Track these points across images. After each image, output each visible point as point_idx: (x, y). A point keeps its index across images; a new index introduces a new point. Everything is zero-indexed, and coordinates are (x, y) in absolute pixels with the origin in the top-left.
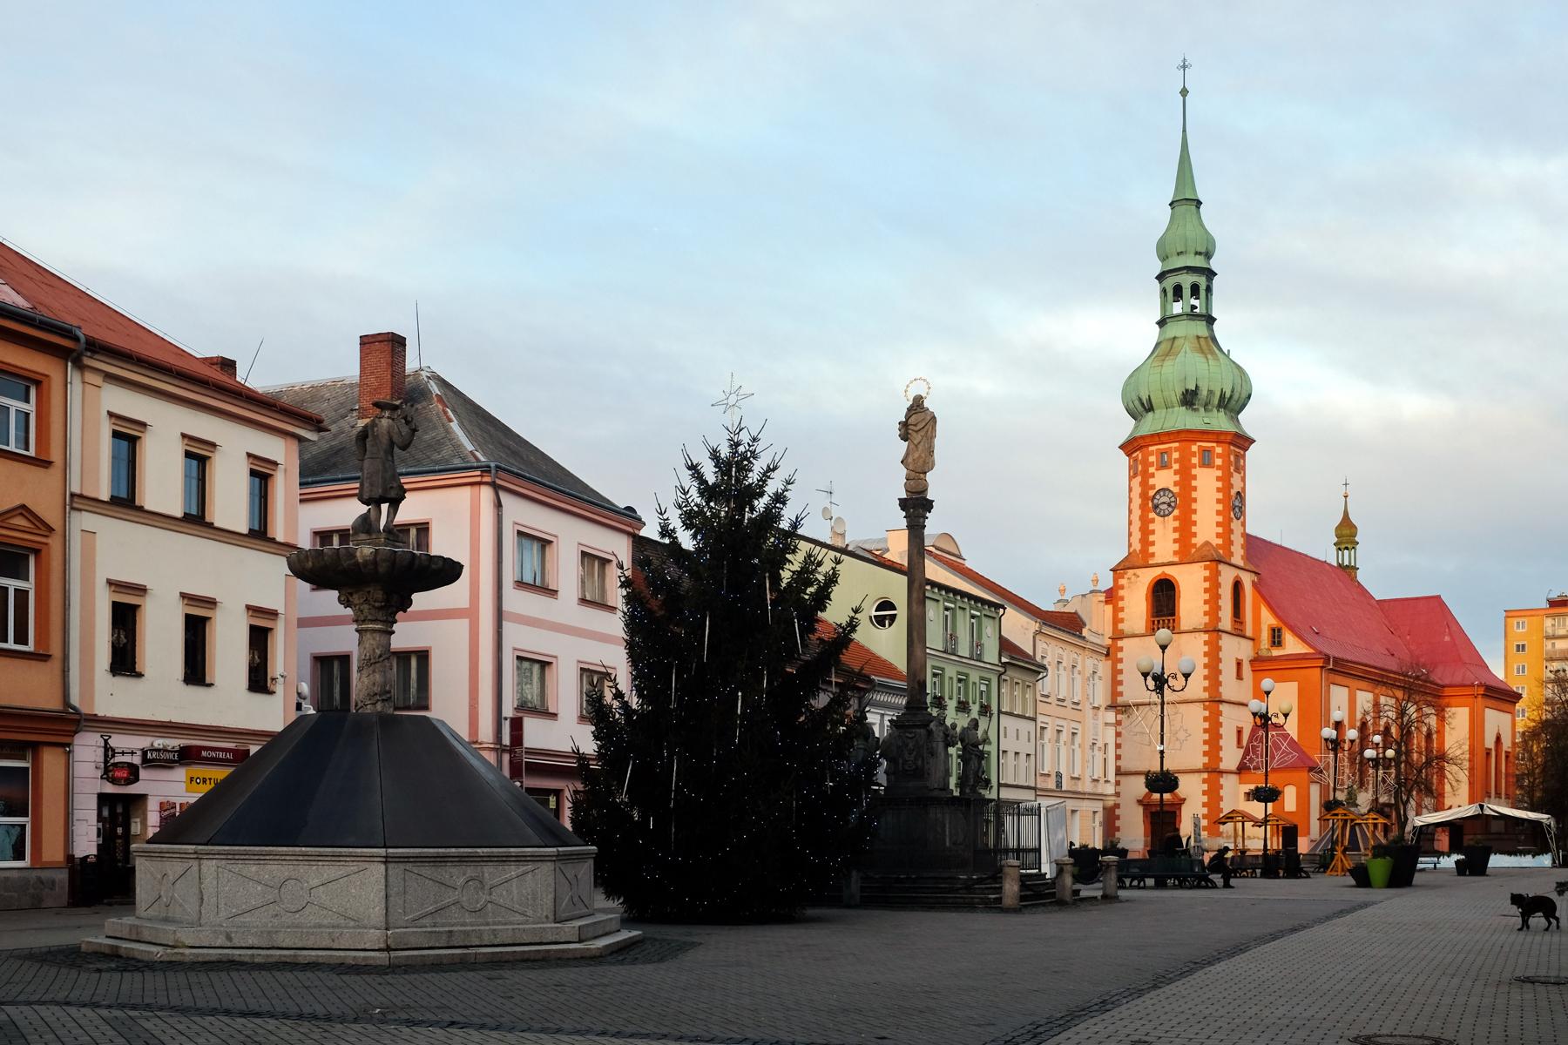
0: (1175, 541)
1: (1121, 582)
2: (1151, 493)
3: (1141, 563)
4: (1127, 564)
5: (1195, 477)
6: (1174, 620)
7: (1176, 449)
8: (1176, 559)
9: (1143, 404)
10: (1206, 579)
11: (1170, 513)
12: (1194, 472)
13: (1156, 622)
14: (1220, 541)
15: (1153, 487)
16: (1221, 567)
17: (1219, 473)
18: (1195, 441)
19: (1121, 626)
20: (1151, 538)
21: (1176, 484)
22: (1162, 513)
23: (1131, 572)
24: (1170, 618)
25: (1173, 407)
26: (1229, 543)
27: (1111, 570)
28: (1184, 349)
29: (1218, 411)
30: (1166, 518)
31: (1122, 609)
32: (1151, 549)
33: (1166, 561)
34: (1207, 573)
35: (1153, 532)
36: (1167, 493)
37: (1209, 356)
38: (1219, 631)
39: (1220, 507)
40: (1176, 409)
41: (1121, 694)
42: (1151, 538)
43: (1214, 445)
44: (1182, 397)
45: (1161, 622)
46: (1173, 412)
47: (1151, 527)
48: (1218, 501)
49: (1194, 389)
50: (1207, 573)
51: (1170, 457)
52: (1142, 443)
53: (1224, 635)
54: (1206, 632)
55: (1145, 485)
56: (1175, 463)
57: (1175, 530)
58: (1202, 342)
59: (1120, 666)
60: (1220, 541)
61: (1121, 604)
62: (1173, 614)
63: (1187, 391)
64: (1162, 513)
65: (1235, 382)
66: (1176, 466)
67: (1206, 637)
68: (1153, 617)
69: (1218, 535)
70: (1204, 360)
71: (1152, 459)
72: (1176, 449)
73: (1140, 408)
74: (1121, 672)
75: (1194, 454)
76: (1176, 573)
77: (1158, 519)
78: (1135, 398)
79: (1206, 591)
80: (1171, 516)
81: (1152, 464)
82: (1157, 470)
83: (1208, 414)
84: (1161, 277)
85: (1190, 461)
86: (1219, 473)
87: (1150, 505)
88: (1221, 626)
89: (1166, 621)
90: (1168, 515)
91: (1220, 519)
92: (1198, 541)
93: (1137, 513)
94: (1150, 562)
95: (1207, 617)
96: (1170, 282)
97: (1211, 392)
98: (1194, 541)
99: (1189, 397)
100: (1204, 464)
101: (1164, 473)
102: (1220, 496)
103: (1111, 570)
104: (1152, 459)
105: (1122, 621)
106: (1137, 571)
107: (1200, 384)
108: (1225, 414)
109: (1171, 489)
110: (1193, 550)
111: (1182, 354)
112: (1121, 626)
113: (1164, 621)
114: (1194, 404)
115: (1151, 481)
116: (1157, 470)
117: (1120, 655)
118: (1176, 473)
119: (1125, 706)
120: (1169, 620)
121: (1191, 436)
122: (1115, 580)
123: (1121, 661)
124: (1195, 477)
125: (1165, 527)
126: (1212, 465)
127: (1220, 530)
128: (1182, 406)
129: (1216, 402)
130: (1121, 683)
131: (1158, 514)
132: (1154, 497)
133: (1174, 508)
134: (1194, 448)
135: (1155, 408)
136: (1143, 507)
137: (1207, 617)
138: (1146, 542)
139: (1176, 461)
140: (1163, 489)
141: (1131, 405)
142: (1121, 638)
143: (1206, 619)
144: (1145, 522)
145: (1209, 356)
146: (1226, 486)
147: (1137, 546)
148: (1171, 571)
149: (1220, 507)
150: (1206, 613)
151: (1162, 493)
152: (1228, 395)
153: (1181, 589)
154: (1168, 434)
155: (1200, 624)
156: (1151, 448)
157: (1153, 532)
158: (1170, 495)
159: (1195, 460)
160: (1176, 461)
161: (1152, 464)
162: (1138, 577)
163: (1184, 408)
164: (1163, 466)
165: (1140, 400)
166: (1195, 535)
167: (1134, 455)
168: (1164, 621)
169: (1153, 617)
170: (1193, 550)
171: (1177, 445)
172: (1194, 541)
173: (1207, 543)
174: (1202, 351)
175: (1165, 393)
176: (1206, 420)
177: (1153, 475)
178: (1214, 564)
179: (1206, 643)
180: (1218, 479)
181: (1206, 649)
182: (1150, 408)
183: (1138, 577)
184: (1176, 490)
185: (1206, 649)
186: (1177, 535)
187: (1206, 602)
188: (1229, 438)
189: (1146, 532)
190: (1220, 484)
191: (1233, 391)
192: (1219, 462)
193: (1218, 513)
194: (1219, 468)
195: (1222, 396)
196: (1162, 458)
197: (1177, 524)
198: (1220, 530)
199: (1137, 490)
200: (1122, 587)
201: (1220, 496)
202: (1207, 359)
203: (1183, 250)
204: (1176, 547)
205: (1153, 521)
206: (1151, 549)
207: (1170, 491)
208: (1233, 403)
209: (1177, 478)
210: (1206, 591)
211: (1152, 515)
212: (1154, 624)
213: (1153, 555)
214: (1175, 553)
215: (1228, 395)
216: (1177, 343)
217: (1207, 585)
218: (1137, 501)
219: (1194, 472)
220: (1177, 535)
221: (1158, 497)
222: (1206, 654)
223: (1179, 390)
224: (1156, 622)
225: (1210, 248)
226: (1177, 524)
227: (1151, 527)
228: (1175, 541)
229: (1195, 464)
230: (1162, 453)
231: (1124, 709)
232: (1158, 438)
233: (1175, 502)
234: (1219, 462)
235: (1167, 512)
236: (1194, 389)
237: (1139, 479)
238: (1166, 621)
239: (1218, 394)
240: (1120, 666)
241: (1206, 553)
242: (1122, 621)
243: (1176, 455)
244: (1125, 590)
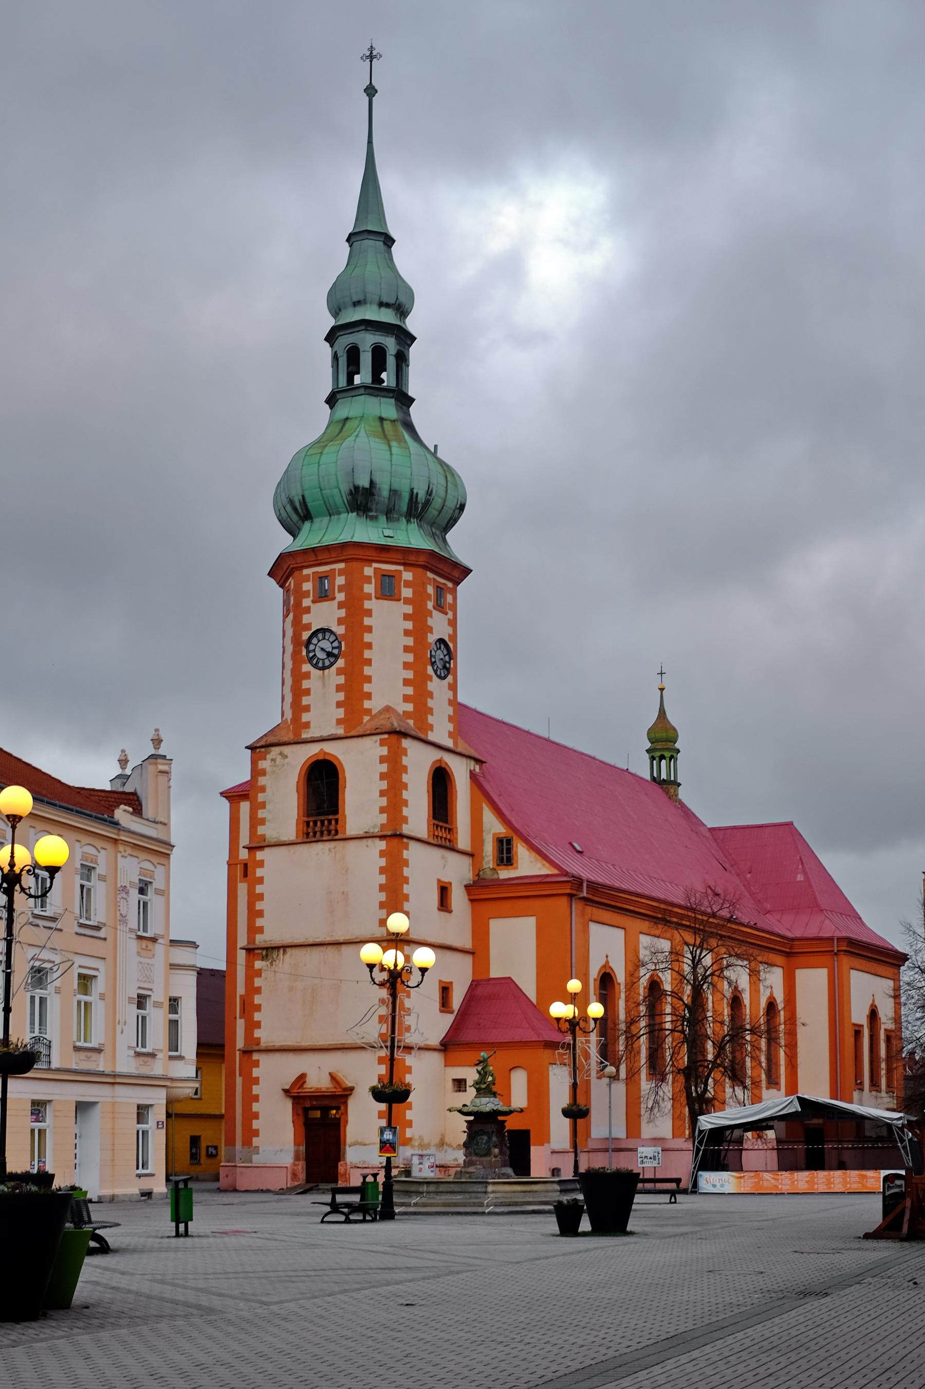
0: (339, 705)
1: (263, 764)
2: (305, 635)
3: (290, 737)
4: (271, 739)
5: (369, 613)
6: (337, 821)
7: (342, 572)
8: (340, 731)
9: (295, 509)
10: (382, 760)
11: (332, 664)
12: (367, 605)
13: (311, 824)
14: (409, 707)
15: (308, 627)
16: (406, 743)
17: (409, 609)
18: (369, 561)
19: (261, 830)
20: (305, 701)
21: (340, 621)
22: (320, 665)
23: (275, 751)
24: (330, 817)
25: (339, 513)
26: (422, 709)
27: (247, 747)
28: (356, 433)
29: (408, 521)
30: (326, 671)
31: (263, 805)
32: (305, 717)
33: (325, 733)
34: (384, 751)
35: (307, 692)
36: (327, 635)
37: (394, 444)
38: (402, 836)
39: (410, 658)
40: (344, 516)
41: (261, 930)
42: (305, 701)
43: (401, 568)
44: (349, 497)
45: (319, 824)
46: (339, 519)
47: (305, 684)
48: (407, 649)
49: (367, 485)
50: (384, 751)
51: (332, 584)
52: (292, 563)
53: (412, 845)
54: (382, 837)
55: (298, 626)
56: (340, 591)
57: (339, 688)
58: (387, 425)
59: (259, 889)
60: (409, 707)
61: (261, 797)
62: (336, 812)
63: (356, 488)
64: (320, 665)
65: (434, 481)
66: (341, 597)
67: (382, 845)
68: (308, 816)
69: (406, 699)
70: (386, 447)
71: (307, 586)
72: (342, 572)
73: (295, 517)
74: (261, 897)
75: (368, 580)
77: (315, 673)
78: (285, 501)
79: (383, 776)
80: (334, 668)
81: (306, 594)
82: (314, 602)
83: (390, 525)
84: (331, 337)
85: (362, 589)
86: (409, 609)
87: (304, 653)
88: (406, 829)
89: (326, 822)
90: (329, 667)
91: (410, 675)
92: (374, 704)
93: (289, 665)
94: (305, 736)
95: (385, 815)
96: (344, 341)
97: (394, 493)
98: (367, 704)
99: (360, 499)
100: (378, 596)
101: (325, 605)
102: (410, 641)
103: (247, 747)
104: (307, 586)
105: (263, 822)
106: (286, 750)
107: (377, 479)
108: (420, 526)
109: (334, 629)
110: (366, 718)
111: (352, 438)
112: (261, 830)
113: (322, 822)
114: (370, 510)
115: (306, 619)
116: (314, 602)
117: (259, 872)
118: (341, 605)
119: (267, 949)
120: (330, 821)
121: (360, 553)
122: (254, 763)
123: (261, 881)
124: (369, 613)
125: (324, 685)
126: (397, 597)
127: (410, 691)
128: (352, 512)
129: (404, 507)
130: (260, 914)
131: (315, 666)
132: (309, 641)
133: (336, 657)
134: (368, 571)
135: (313, 516)
136: (296, 655)
137: (385, 815)
138: (298, 708)
139: (341, 589)
140: (323, 631)
141: (284, 515)
142: (261, 848)
143: (383, 818)
144: (298, 677)
145: (394, 444)
146: (419, 629)
147: (289, 715)
148: (332, 749)
149: (410, 658)
150: (382, 810)
151: (320, 636)
152: (422, 496)
153: (347, 774)
154: (328, 548)
155: (374, 827)
156: (306, 572)
157: (307, 692)
158: (332, 638)
159: (369, 588)
160: (341, 589)
161: (306, 594)
162: (286, 757)
163: (355, 514)
164: (323, 596)
165: (291, 502)
166: (369, 696)
167: (287, 585)
168: (322, 822)
170: (366, 718)
171: (342, 565)
172: (367, 704)
173: (388, 709)
174: (385, 436)
175: (327, 492)
176: (387, 532)
177: (308, 610)
178: (394, 738)
179: (382, 854)
180: (406, 617)
181: (383, 862)
182: (307, 516)
183: (286, 757)
184: (340, 630)
185: (383, 862)
186: (341, 696)
187: (382, 793)
188: (422, 560)
189: (299, 692)
190: (409, 625)
191: (429, 493)
192: (407, 593)
193: (406, 666)
194: (407, 601)
195: (413, 497)
196: (322, 584)
197: (341, 680)
198: (410, 691)
199: (290, 632)
200: (263, 773)
201: (410, 641)
202: (390, 447)
203: (361, 298)
204: (341, 713)
205: (307, 675)
206: (305, 717)
207: (332, 632)
209: (342, 613)
210: (383, 776)
211: (306, 667)
212: (308, 825)
213: (307, 725)
214: (339, 722)
215: (422, 496)
216: (349, 425)
217: (384, 768)
218: (290, 648)
219: (367, 605)
220: (341, 696)
221: (315, 641)
222: (382, 870)
223: (345, 488)
224: (311, 824)
226: (341, 680)
227: (305, 684)
228: (339, 705)
229: (370, 595)
230: (321, 578)
231: (264, 953)
232: (316, 555)
233: (339, 647)
234: (407, 593)
235: (327, 663)
236: (367, 485)
237: (291, 616)
238: (326, 822)
239: (406, 496)
240: (259, 889)
241: (383, 722)
242: (263, 822)
243: (340, 581)
244: (267, 777)
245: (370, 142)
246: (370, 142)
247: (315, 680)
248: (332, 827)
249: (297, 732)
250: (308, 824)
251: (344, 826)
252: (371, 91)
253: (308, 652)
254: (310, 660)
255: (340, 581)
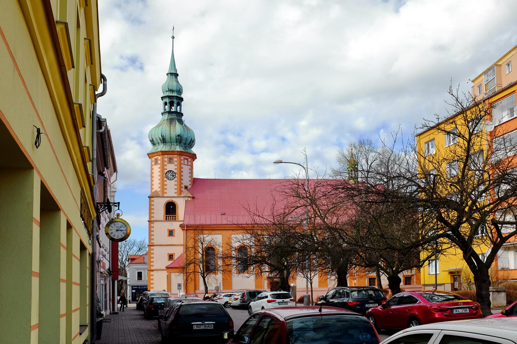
2: (166, 171)
3: (161, 195)
5: (182, 168)
6: (175, 217)
8: (176, 195)
11: (173, 179)
15: (166, 169)
21: (175, 169)
22: (170, 179)
47: (165, 183)
62: (176, 215)
71: (166, 159)
76: (176, 200)
81: (166, 161)
82: (168, 163)
90: (172, 180)
94: (165, 195)
115: (165, 167)
116: (168, 163)
118: (175, 165)
120: (173, 217)
124: (182, 168)
131: (168, 179)
132: (166, 173)
133: (175, 178)
140: (170, 171)
156: (165, 156)
161: (166, 161)
169: (166, 214)
177: (166, 165)
184: (176, 171)
205: (166, 181)
207: (173, 171)
208: (191, 143)
211: (165, 179)
214: (175, 193)
225: (181, 88)
227: (165, 183)
233: (175, 175)
235: (172, 179)
245: (173, 50)
246: (173, 50)
247: (168, 182)
248: (174, 218)
249: (163, 194)
250: (166, 217)
251: (178, 218)
252: (173, 38)
253: (166, 175)
254: (167, 177)
255: (175, 159)
